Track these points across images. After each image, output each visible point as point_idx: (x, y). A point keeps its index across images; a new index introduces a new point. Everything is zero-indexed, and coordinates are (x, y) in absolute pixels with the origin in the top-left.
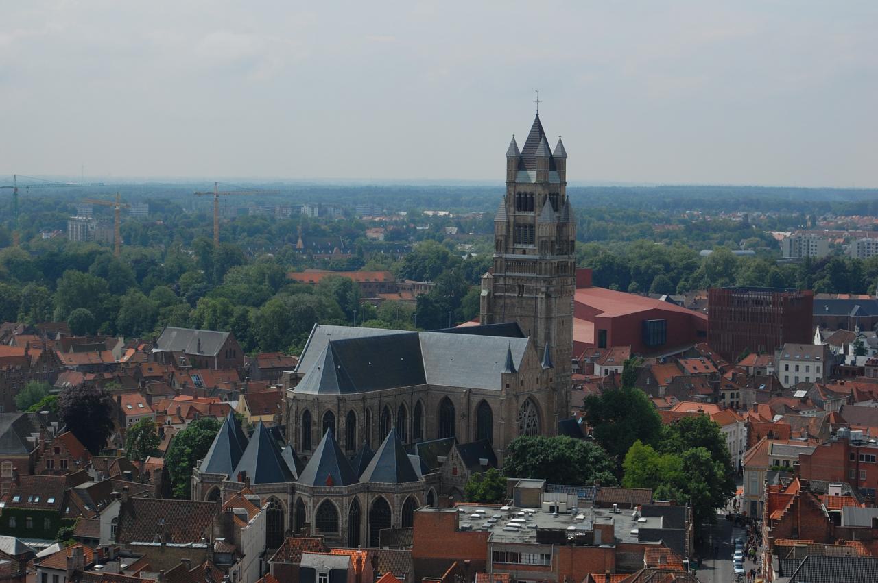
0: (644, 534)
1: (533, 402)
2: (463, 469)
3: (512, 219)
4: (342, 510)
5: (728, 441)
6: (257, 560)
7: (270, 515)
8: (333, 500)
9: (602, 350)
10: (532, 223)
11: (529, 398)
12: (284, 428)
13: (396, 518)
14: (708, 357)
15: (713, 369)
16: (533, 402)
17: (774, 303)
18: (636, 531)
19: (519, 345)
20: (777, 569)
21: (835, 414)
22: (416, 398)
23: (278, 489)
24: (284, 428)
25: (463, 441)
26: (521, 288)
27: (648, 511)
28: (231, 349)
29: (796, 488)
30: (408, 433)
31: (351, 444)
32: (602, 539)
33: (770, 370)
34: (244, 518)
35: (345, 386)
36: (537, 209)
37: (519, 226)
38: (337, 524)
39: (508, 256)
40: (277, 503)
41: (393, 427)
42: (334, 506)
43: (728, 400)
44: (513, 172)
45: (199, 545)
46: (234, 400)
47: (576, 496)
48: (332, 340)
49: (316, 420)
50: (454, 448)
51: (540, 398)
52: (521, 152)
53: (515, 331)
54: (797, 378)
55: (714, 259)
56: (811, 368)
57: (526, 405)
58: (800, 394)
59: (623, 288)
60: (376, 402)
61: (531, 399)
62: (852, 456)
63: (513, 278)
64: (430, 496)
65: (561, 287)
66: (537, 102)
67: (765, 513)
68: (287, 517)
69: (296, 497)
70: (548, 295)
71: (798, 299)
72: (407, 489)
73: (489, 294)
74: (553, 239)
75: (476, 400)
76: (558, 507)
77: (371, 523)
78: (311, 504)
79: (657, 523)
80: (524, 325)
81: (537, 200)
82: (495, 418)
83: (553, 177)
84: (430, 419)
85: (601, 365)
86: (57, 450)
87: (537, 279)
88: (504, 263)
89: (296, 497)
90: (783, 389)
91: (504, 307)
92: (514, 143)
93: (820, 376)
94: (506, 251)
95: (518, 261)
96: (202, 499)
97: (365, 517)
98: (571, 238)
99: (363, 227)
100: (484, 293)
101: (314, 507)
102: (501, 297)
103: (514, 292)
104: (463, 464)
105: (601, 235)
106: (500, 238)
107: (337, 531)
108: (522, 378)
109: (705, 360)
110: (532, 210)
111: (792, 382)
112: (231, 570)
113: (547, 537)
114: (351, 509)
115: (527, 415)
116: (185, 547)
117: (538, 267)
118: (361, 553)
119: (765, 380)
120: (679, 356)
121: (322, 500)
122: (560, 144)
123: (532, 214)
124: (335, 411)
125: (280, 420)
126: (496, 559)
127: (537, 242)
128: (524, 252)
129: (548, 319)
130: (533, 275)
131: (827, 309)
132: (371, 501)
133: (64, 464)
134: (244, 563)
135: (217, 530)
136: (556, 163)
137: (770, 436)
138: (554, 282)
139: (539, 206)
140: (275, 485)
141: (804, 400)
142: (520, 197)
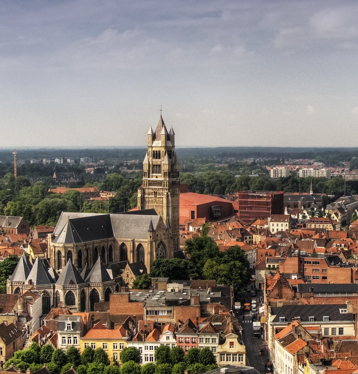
0: (213, 300)
1: (162, 244)
5: (249, 257)
6: (38, 319)
9: (193, 220)
10: (160, 164)
13: (101, 298)
14: (239, 221)
15: (241, 227)
16: (162, 244)
17: (267, 197)
19: (155, 219)
20: (270, 312)
21: (294, 244)
22: (109, 243)
23: (47, 287)
27: (214, 289)
28: (23, 224)
29: (277, 277)
30: (106, 260)
32: (194, 303)
33: (266, 226)
35: (77, 240)
36: (162, 158)
37: (154, 166)
38: (75, 301)
39: (150, 179)
40: (47, 293)
41: (99, 257)
42: (73, 294)
43: (248, 240)
44: (151, 141)
45: (11, 314)
46: (26, 247)
47: (183, 285)
48: (70, 218)
49: (64, 255)
50: (127, 265)
53: (152, 212)
54: (277, 229)
55: (241, 178)
56: (284, 225)
57: (159, 245)
59: (202, 192)
60: (91, 246)
61: (161, 242)
62: (301, 262)
65: (174, 192)
67: (265, 288)
72: (106, 284)
73: (141, 196)
74: (170, 171)
75: (137, 244)
76: (174, 290)
77: (91, 300)
79: (219, 295)
84: (116, 253)
88: (148, 183)
93: (287, 228)
94: (149, 177)
95: (154, 181)
97: (87, 298)
98: (177, 171)
99: (84, 167)
101: (64, 294)
102: (147, 197)
103: (153, 195)
104: (132, 272)
105: (191, 169)
106: (146, 171)
107: (75, 305)
108: (157, 233)
109: (238, 222)
110: (159, 158)
111: (275, 231)
113: (171, 303)
114: (81, 295)
115: (160, 249)
116: (5, 315)
118: (86, 314)
119: (264, 230)
121: (67, 291)
123: (160, 160)
125: (47, 256)
126: (147, 314)
127: (162, 172)
128: (157, 177)
129: (168, 207)
130: (161, 187)
131: (290, 199)
132: (90, 291)
136: (169, 137)
138: (170, 190)
139: (163, 156)
140: (46, 285)
142: (154, 153)
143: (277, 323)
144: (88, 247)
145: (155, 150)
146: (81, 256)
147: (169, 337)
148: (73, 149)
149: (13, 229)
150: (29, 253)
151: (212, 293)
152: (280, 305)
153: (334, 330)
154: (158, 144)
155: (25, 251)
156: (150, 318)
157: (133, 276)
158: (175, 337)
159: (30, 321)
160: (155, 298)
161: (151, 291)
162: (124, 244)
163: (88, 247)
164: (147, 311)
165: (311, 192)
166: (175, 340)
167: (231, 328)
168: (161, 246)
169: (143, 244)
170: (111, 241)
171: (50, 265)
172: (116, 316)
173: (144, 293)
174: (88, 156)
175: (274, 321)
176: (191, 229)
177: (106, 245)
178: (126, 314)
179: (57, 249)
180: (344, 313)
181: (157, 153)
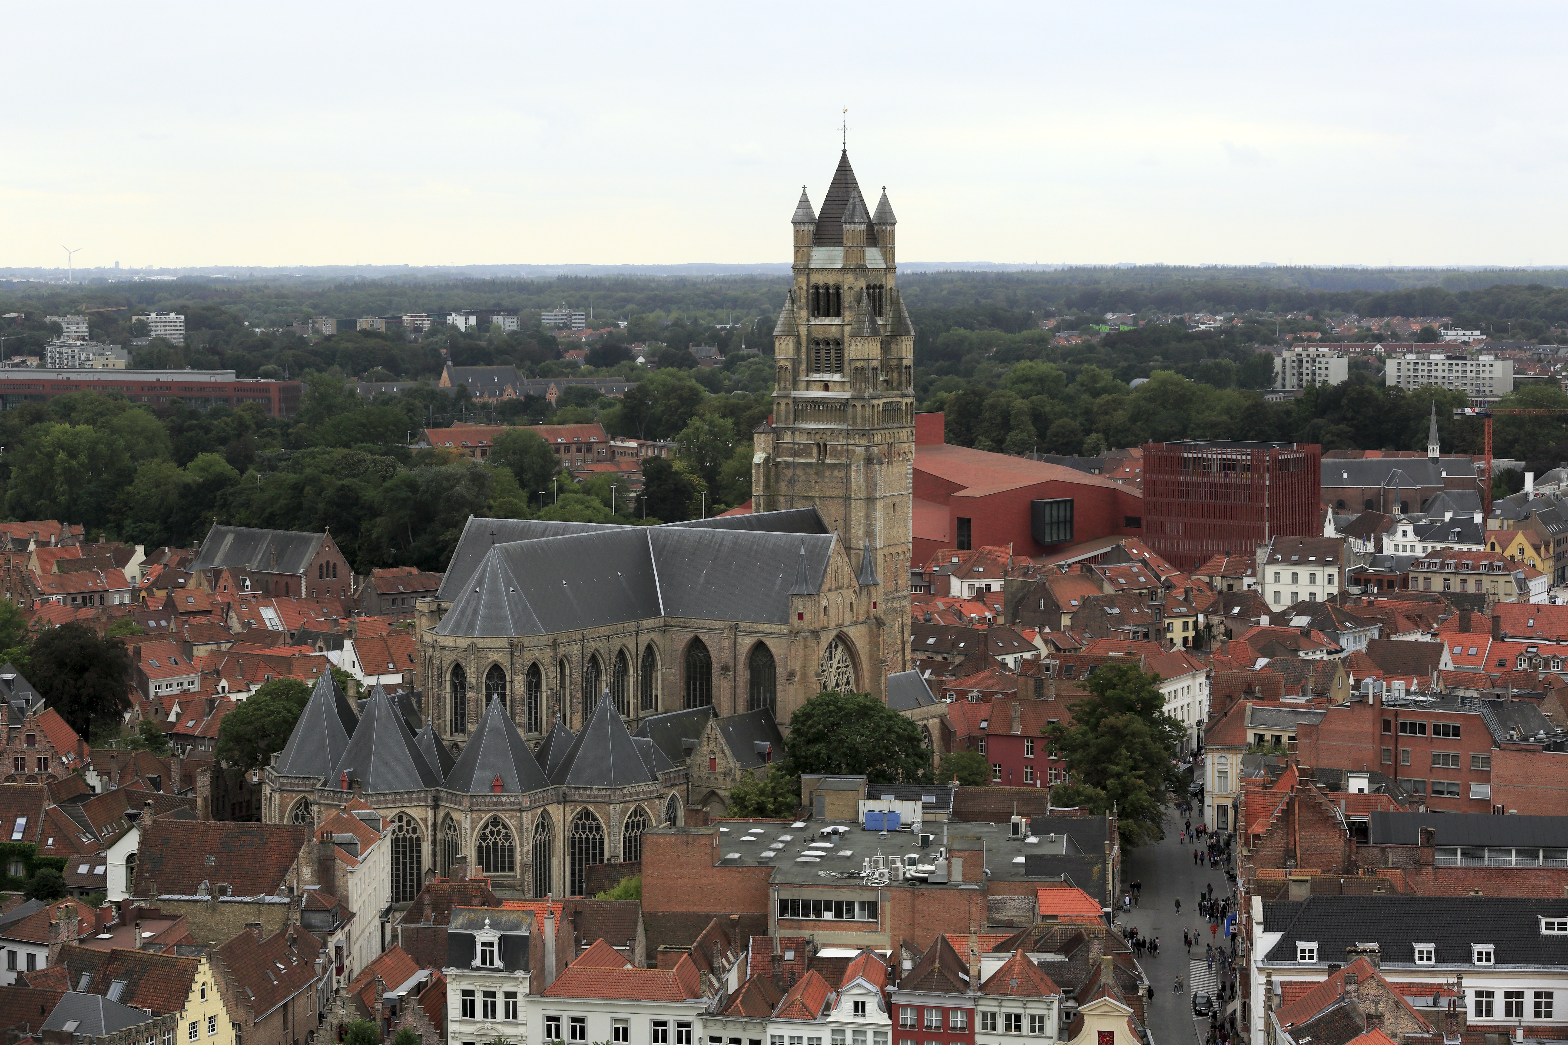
1: (844, 643)
2: (728, 761)
3: (803, 330)
4: (520, 833)
6: (377, 922)
7: (395, 842)
8: (504, 817)
10: (838, 336)
11: (838, 636)
12: (419, 696)
18: (1021, 859)
22: (644, 640)
24: (419, 696)
25: (725, 711)
26: (822, 448)
28: (328, 562)
30: (631, 701)
31: (533, 723)
32: (964, 875)
34: (350, 847)
45: (276, 899)
46: (334, 649)
47: (919, 804)
51: (858, 635)
52: (817, 212)
57: (832, 647)
58: (1301, 621)
59: (999, 447)
61: (842, 639)
62: (1387, 725)
63: (809, 432)
64: (672, 805)
66: (844, 129)
68: (426, 848)
69: (441, 813)
70: (869, 460)
71: (1295, 460)
72: (631, 795)
73: (767, 460)
74: (875, 363)
78: (466, 824)
79: (1060, 846)
80: (829, 513)
81: (848, 298)
82: (781, 673)
83: (873, 258)
85: (963, 577)
86: (31, 740)
87: (848, 434)
88: (791, 406)
89: (441, 813)
90: (1268, 611)
91: (792, 482)
92: (804, 202)
96: (281, 818)
97: (559, 846)
98: (906, 362)
100: (759, 457)
101: (473, 829)
102: (788, 465)
103: (810, 455)
106: (783, 363)
110: (838, 314)
111: (1286, 602)
112: (332, 942)
115: (835, 666)
117: (850, 410)
120: (1094, 560)
121: (486, 817)
122: (884, 203)
123: (837, 321)
124: (505, 663)
126: (783, 911)
127: (847, 369)
128: (826, 387)
130: (845, 427)
132: (569, 818)
133: (42, 764)
134: (355, 926)
135: (307, 872)
137: (1249, 692)
138: (878, 438)
141: (1306, 633)
143: (1288, 965)
144: (562, 650)
145: (821, 283)
146: (538, 685)
147: (863, 1003)
148: (513, 276)
149: (289, 579)
150: (347, 668)
151: (1032, 840)
152: (1299, 893)
153: (1514, 999)
154: (832, 259)
155: (335, 662)
156: (790, 928)
157: (732, 764)
158: (890, 1009)
159: (346, 929)
160: (813, 853)
161: (799, 824)
162: (701, 641)
163: (562, 650)
164: (783, 905)
165: (1430, 447)
166: (886, 1015)
167: (1107, 977)
168: (839, 653)
169: (770, 643)
170: (650, 630)
171: (423, 718)
172: (664, 916)
173: (772, 830)
174: (570, 306)
175: (1272, 956)
176: (959, 588)
177: (631, 646)
178: (703, 910)
179: (448, 659)
180: (1556, 932)
181: (828, 293)
